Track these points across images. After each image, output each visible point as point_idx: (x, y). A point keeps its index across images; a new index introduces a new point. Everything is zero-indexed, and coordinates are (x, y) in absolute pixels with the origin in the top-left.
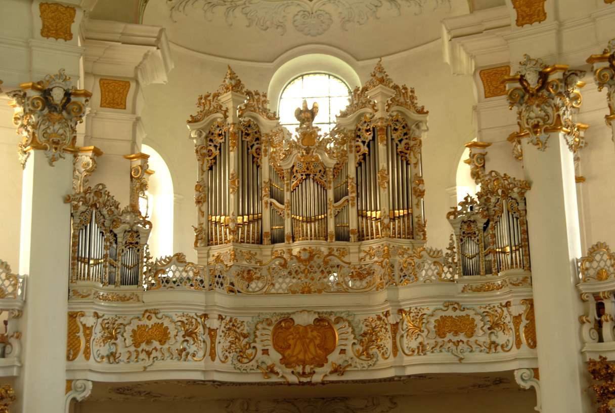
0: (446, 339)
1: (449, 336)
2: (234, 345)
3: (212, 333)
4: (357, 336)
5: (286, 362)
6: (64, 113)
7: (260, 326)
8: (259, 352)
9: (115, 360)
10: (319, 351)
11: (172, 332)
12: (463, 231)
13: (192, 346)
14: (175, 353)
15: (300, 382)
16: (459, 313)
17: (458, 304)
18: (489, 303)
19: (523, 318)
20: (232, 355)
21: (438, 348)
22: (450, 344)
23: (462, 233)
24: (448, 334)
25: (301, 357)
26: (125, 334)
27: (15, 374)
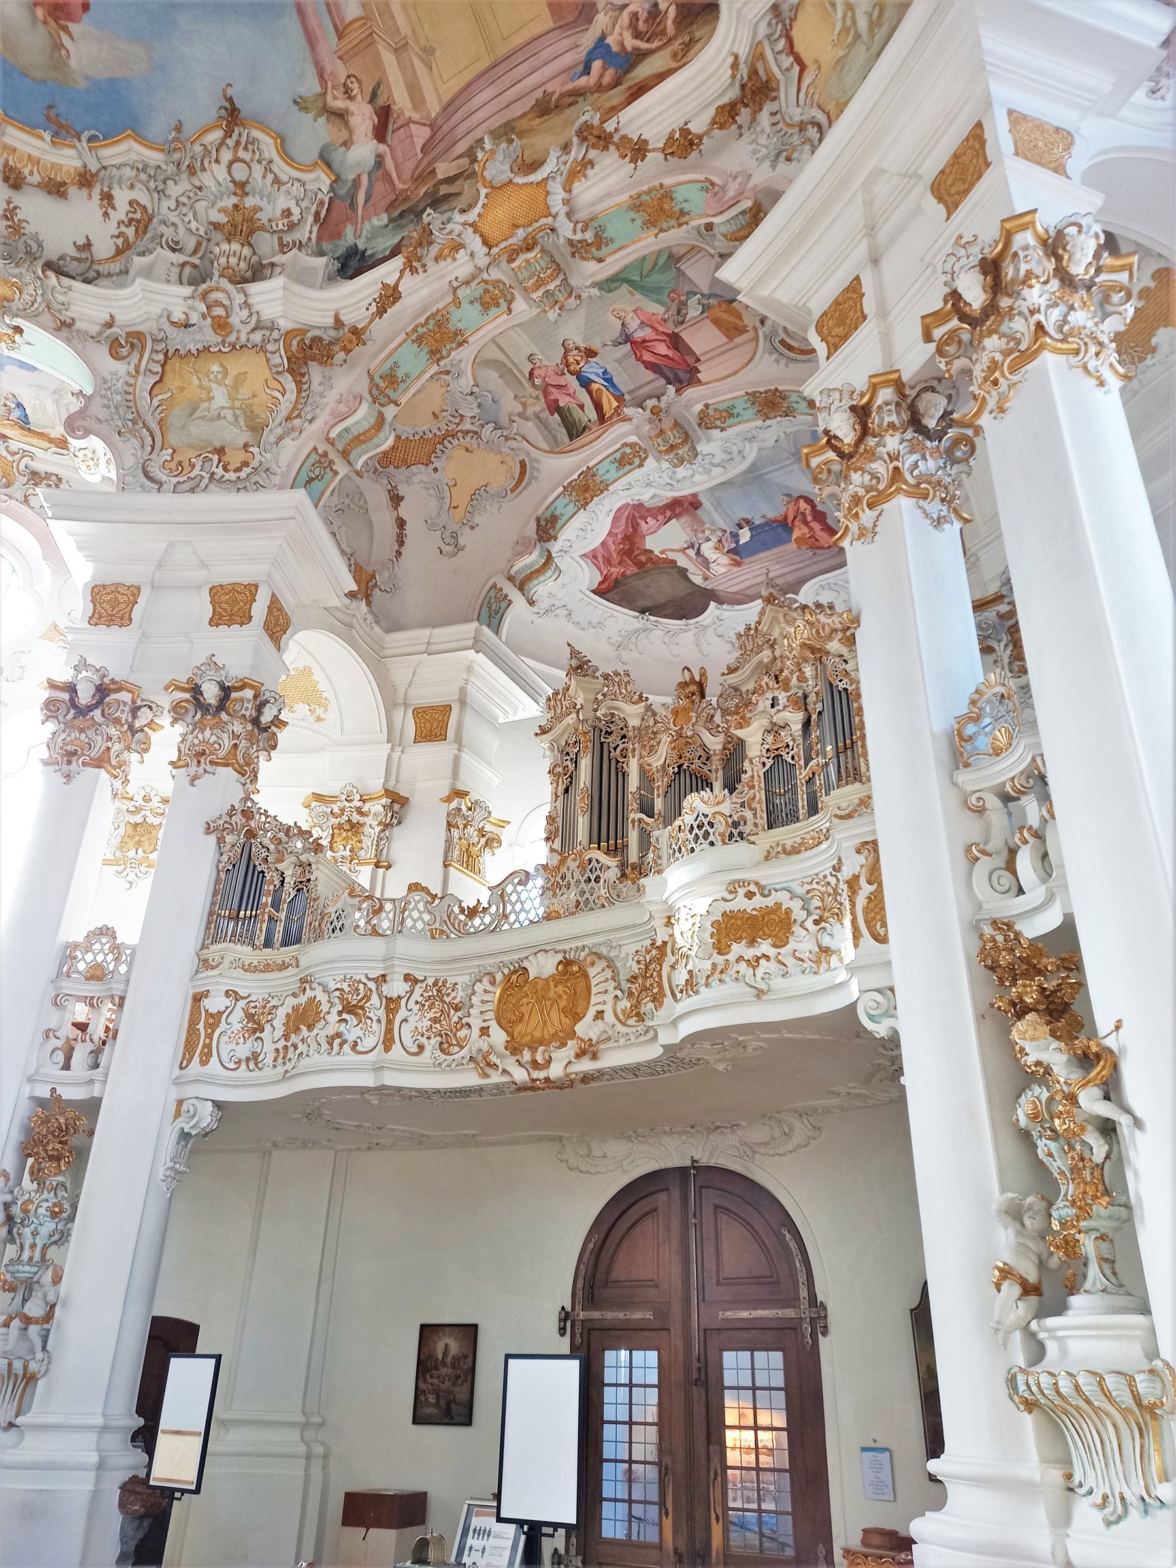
0: (731, 957)
1: (737, 949)
2: (438, 1026)
3: (392, 1005)
4: (623, 983)
5: (514, 1048)
6: (224, 716)
7: (479, 987)
8: (476, 1032)
9: (256, 1065)
10: (564, 1020)
11: (325, 1007)
12: (767, 747)
13: (353, 1029)
14: (325, 1046)
15: (534, 1080)
16: (758, 901)
17: (757, 884)
18: (816, 871)
19: (863, 881)
20: (433, 1041)
21: (717, 975)
22: (743, 966)
23: (764, 751)
24: (735, 946)
25: (538, 1034)
26: (275, 1023)
27: (96, 1095)
